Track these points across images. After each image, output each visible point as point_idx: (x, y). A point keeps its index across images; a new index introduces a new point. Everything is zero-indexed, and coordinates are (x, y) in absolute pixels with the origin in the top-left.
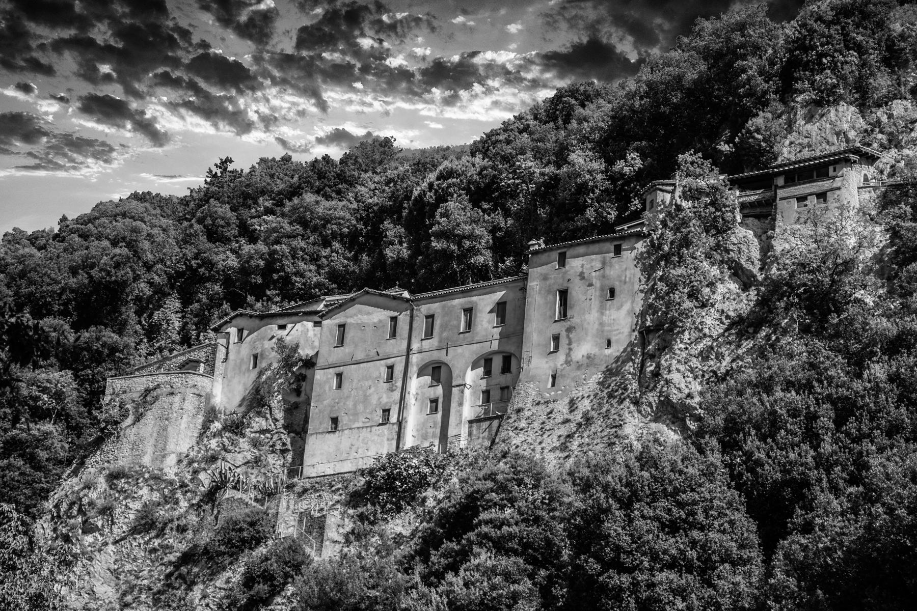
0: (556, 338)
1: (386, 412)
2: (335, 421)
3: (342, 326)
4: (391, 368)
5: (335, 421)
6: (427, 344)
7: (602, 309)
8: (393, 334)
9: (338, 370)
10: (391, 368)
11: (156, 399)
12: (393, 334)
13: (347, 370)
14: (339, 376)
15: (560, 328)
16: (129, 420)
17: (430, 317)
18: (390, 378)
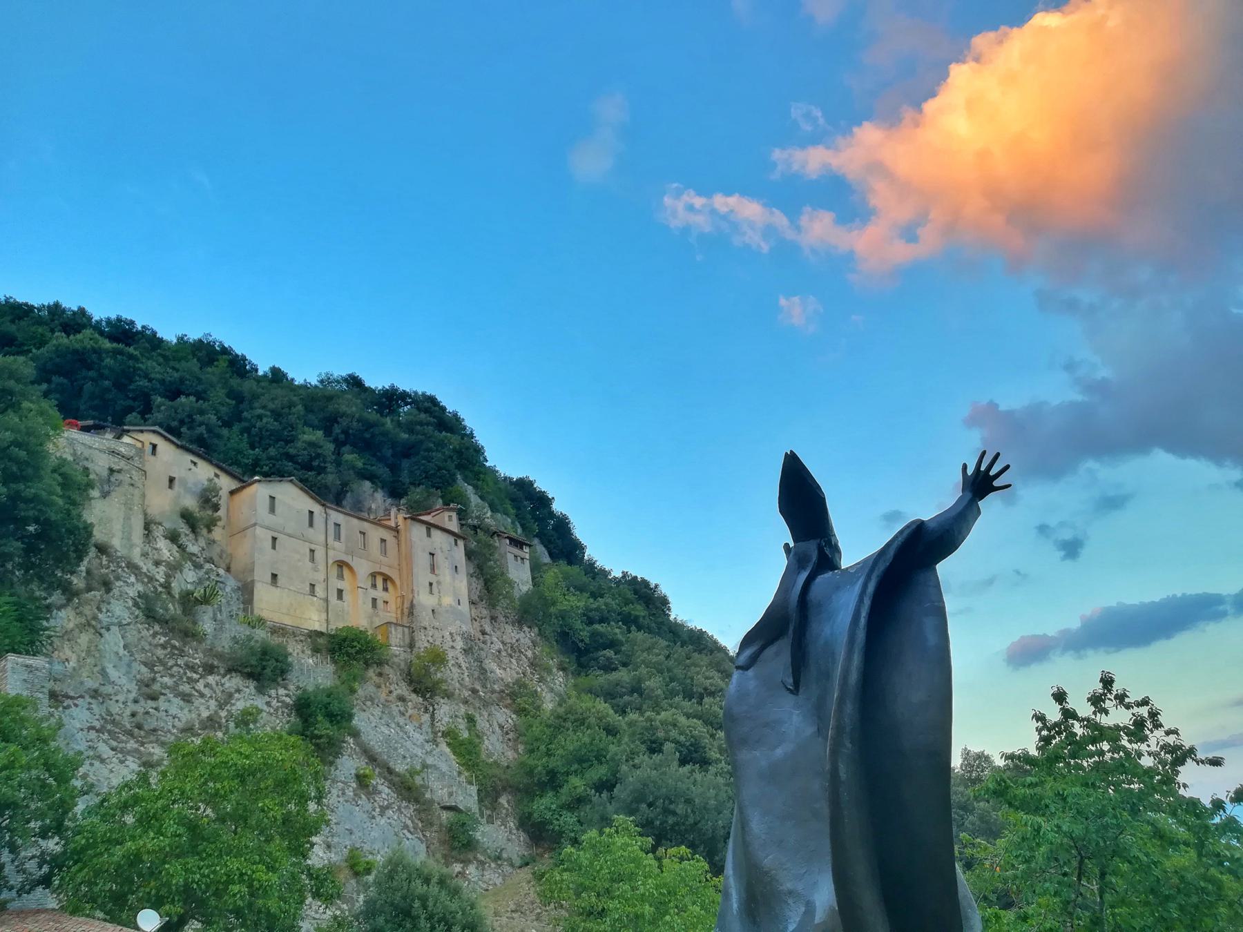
0: (431, 584)
1: (313, 586)
2: (274, 576)
3: (272, 498)
4: (312, 551)
5: (274, 576)
6: (337, 544)
7: (454, 578)
8: (311, 524)
9: (275, 535)
10: (312, 551)
11: (120, 484)
12: (311, 524)
13: (281, 537)
14: (274, 539)
15: (433, 578)
16: (95, 493)
17: (337, 525)
18: (312, 559)
